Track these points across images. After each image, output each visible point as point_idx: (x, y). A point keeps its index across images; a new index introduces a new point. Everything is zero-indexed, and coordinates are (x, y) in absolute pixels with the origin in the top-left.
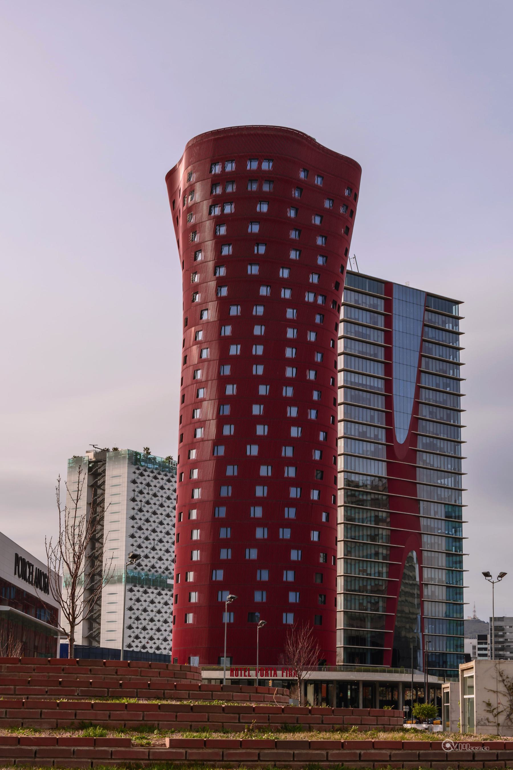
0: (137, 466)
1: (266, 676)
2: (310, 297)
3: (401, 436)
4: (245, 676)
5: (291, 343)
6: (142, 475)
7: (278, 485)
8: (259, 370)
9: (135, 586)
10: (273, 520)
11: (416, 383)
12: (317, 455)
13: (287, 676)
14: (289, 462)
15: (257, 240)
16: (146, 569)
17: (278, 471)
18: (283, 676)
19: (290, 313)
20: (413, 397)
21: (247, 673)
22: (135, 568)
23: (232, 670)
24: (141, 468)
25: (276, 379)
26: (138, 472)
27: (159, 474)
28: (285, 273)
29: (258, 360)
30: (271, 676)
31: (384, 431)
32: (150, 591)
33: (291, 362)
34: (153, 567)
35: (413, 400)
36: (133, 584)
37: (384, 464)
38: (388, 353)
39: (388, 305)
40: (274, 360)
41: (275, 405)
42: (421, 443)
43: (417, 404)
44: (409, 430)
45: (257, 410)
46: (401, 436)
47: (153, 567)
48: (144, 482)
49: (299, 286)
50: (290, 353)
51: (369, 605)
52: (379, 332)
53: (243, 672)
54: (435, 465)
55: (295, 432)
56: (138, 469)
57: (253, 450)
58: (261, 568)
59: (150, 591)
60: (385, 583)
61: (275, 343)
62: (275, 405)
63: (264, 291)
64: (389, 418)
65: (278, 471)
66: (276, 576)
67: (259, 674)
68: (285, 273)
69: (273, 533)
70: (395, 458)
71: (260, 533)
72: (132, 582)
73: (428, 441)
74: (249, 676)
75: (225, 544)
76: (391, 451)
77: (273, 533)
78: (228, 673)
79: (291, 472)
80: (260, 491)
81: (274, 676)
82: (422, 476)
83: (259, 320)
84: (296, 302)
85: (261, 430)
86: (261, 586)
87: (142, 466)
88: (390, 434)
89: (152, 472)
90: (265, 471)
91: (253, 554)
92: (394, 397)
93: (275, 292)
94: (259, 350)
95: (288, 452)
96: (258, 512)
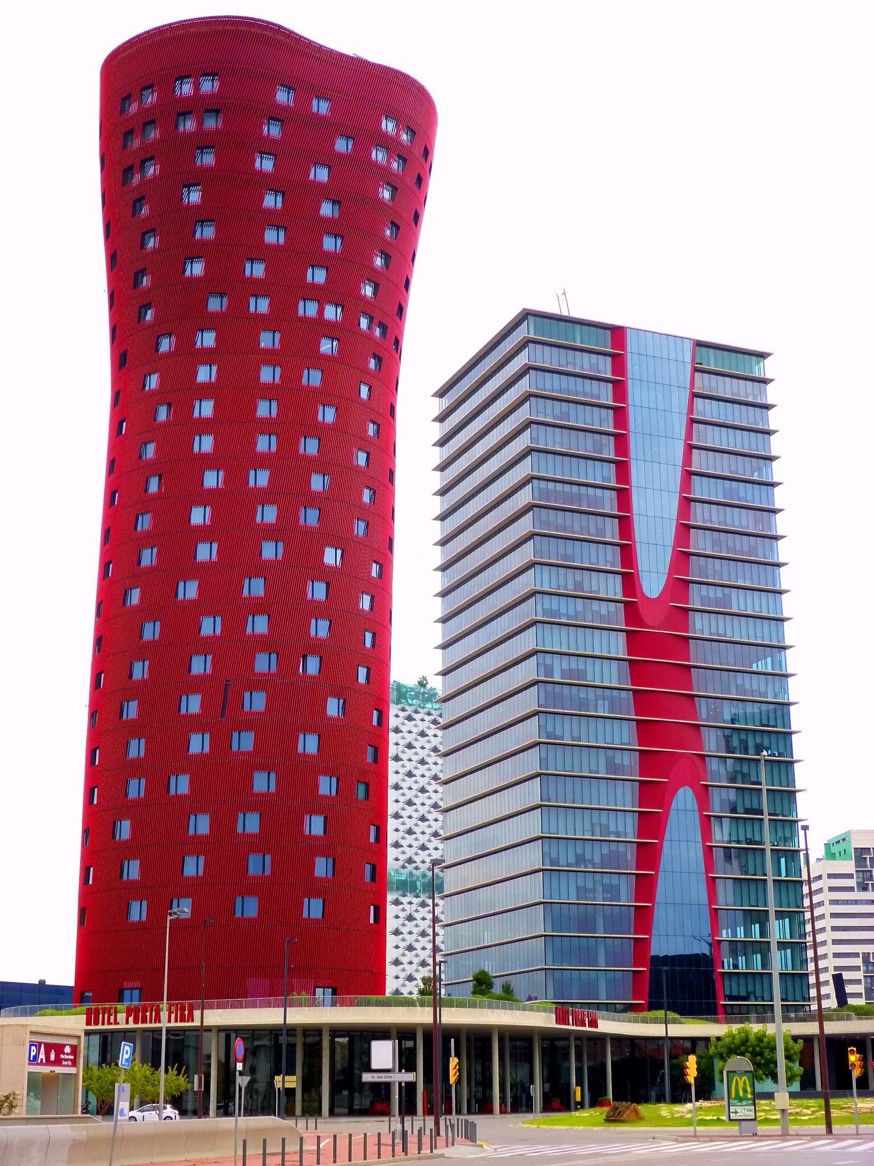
0: (400, 706)
1: (142, 1022)
2: (310, 309)
4: (109, 1023)
6: (410, 718)
7: (234, 649)
8: (205, 444)
9: (404, 895)
10: (222, 716)
11: (681, 493)
12: (365, 602)
13: (176, 1021)
14: (257, 607)
15: (200, 215)
16: (424, 867)
17: (234, 624)
18: (169, 1021)
19: (267, 340)
20: (674, 514)
21: (112, 1018)
22: (404, 867)
23: (89, 1013)
24: (407, 707)
25: (235, 458)
26: (402, 714)
27: (416, 712)
28: (258, 270)
29: (204, 426)
30: (151, 1022)
32: (404, 900)
33: (267, 426)
34: (410, 861)
35: (674, 523)
36: (400, 892)
37: (622, 636)
38: (622, 443)
39: (619, 363)
40: (235, 423)
41: (234, 504)
42: (697, 598)
43: (684, 530)
44: (669, 575)
45: (199, 516)
47: (410, 861)
48: (415, 730)
49: (286, 287)
50: (265, 409)
51: (600, 889)
52: (604, 411)
53: (106, 1015)
54: (729, 634)
55: (270, 551)
56: (403, 710)
57: (190, 590)
58: (198, 810)
59: (404, 900)
60: (632, 847)
61: (235, 394)
62: (234, 504)
63: (214, 304)
64: (628, 554)
65: (234, 624)
66: (223, 825)
67: (131, 1019)
68: (258, 270)
69: (221, 743)
70: (641, 623)
71: (198, 744)
72: (397, 889)
73: (719, 595)
74: (116, 1023)
75: (137, 768)
76: (632, 612)
77: (221, 743)
78: (84, 1017)
79: (260, 625)
80: (199, 665)
81: (155, 1022)
82: (697, 655)
83: (207, 356)
84: (281, 317)
85: (205, 552)
86: (197, 845)
87: (410, 705)
88: (630, 583)
89: (429, 714)
90: (209, 627)
91: (181, 785)
92: (636, 518)
94: (206, 409)
95: (256, 587)
96: (193, 704)
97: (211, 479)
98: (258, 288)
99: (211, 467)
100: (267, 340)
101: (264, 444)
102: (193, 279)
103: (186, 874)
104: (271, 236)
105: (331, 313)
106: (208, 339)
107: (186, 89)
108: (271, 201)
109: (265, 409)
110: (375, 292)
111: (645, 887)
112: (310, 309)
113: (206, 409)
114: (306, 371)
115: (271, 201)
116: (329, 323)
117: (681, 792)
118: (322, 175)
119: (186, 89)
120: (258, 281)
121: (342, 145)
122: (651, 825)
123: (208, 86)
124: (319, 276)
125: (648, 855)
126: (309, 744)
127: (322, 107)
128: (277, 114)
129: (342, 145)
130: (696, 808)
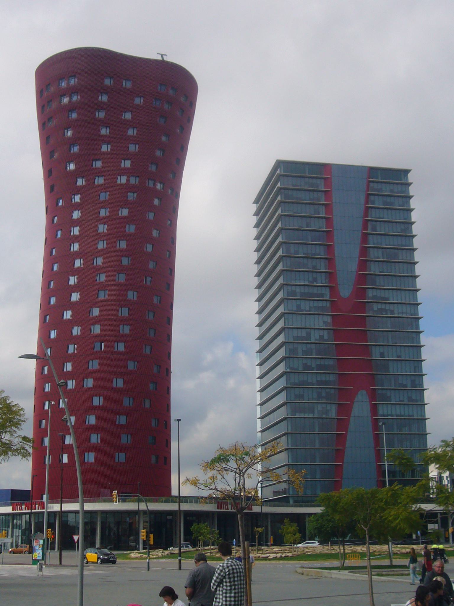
2: (123, 180)
3: (345, 292)
5: (103, 220)
8: (75, 247)
29: (75, 239)
31: (328, 289)
45: (73, 280)
46: (345, 292)
64: (331, 276)
66: (81, 420)
77: (80, 384)
83: (77, 207)
88: (333, 290)
90: (76, 331)
93: (90, 182)
94: (76, 231)
97: (78, 263)
98: (99, 173)
99: (78, 258)
100: (104, 196)
101: (102, 245)
102: (71, 172)
103: (66, 443)
104: (105, 148)
105: (133, 181)
106: (77, 199)
107: (64, 84)
108: (104, 131)
109: (102, 229)
110: (157, 168)
111: (341, 439)
112: (123, 180)
113: (76, 231)
114: (121, 209)
115: (104, 131)
116: (133, 185)
117: (360, 393)
118: (128, 116)
119: (64, 84)
120: (99, 169)
121: (138, 101)
122: (344, 409)
123: (73, 82)
124: (127, 164)
125: (342, 423)
126: (119, 383)
127: (127, 84)
128: (105, 90)
129: (138, 101)
130: (368, 400)
